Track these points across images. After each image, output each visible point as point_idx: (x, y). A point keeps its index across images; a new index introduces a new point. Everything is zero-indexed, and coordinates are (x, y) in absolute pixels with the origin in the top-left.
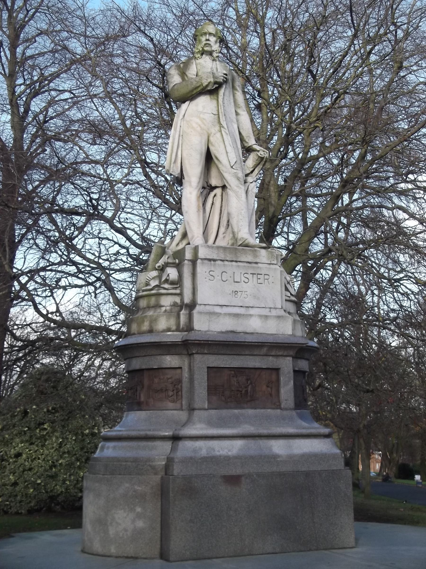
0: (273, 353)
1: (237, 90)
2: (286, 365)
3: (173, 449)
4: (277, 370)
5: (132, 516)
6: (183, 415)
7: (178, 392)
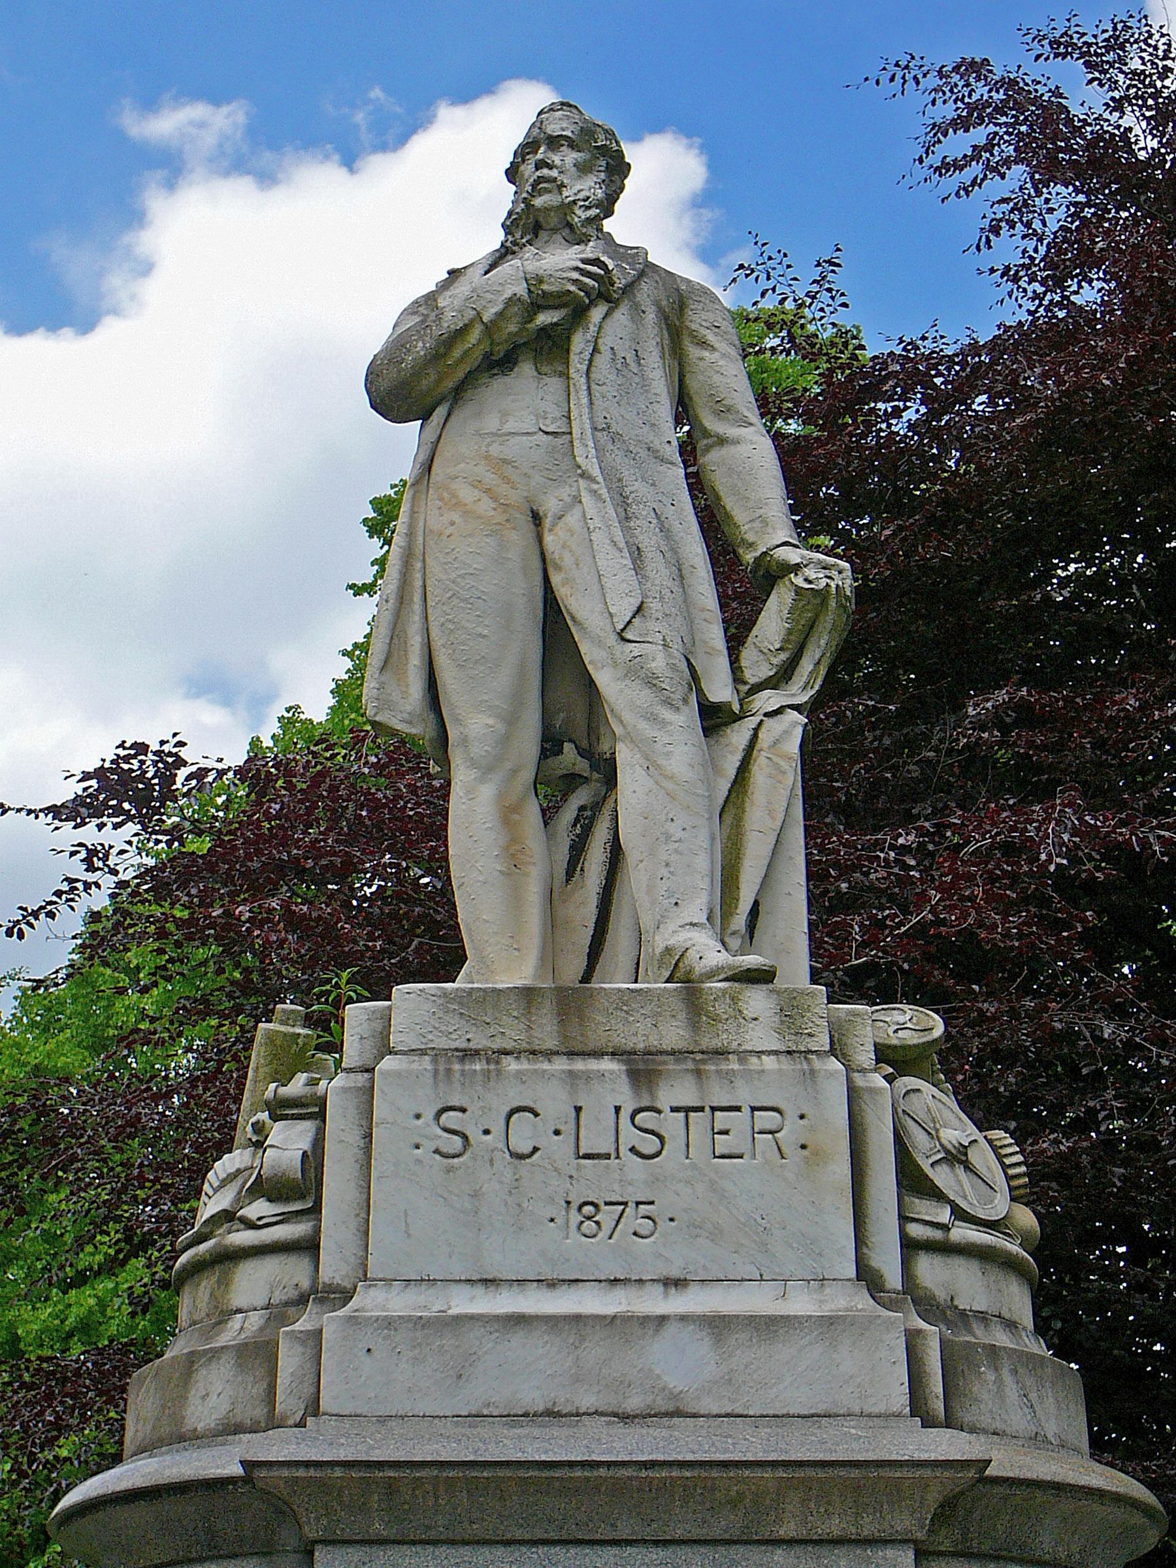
0: (788, 1529)
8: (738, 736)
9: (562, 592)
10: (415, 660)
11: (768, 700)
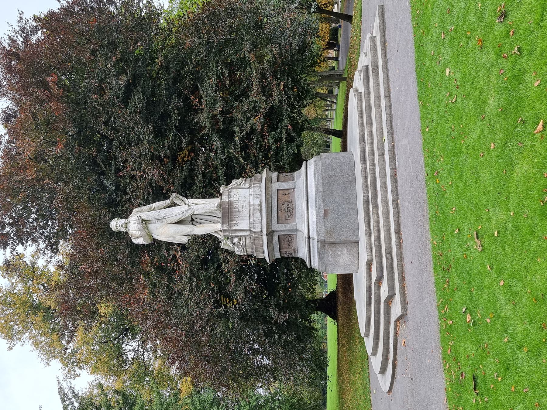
2: (276, 186)
3: (313, 239)
4: (278, 190)
5: (342, 255)
6: (299, 234)
7: (289, 235)
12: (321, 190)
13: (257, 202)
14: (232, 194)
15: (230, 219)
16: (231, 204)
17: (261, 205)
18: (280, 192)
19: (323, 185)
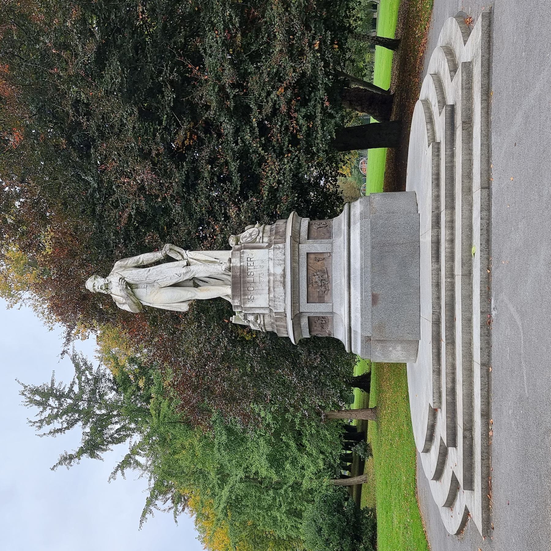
0: (297, 258)
1: (127, 264)
4: (307, 253)
5: (394, 351)
8: (191, 260)
9: (171, 284)
10: (179, 304)
11: (185, 256)
12: (369, 263)
13: (279, 271)
14: (245, 256)
15: (242, 293)
16: (243, 271)
17: (284, 276)
18: (312, 256)
19: (372, 258)
